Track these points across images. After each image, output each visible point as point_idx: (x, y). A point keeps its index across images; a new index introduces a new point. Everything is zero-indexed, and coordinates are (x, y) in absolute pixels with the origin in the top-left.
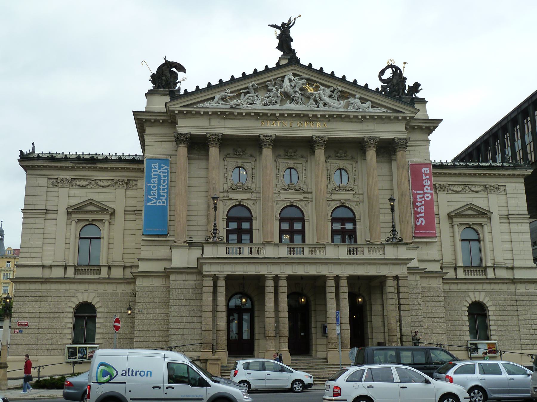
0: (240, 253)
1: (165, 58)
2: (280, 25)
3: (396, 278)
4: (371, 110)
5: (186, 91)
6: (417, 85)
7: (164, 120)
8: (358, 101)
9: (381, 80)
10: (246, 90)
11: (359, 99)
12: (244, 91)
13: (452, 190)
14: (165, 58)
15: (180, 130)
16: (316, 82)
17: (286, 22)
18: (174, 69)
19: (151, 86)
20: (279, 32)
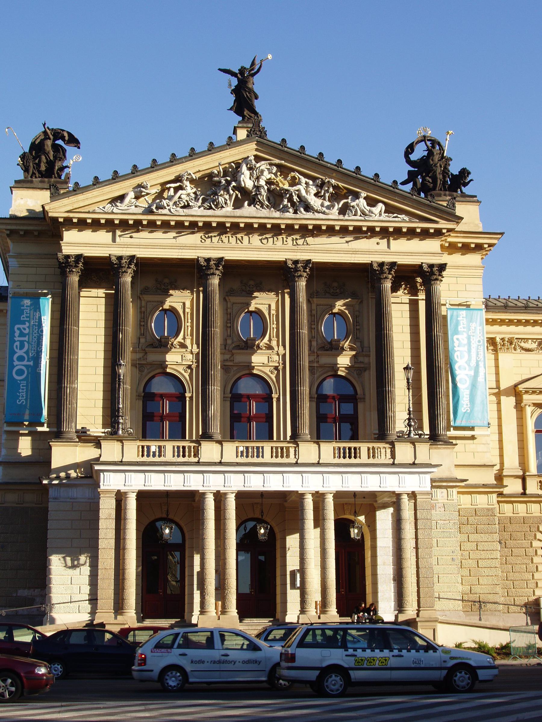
0: (160, 456)
1: (44, 125)
2: (237, 72)
3: (413, 495)
4: (384, 217)
5: (77, 184)
6: (464, 173)
7: (41, 234)
8: (362, 202)
9: (409, 161)
10: (178, 184)
11: (365, 198)
12: (173, 185)
13: (523, 349)
14: (44, 125)
15: (67, 250)
16: (294, 170)
17: (248, 66)
18: (60, 142)
19: (20, 175)
20: (235, 82)
